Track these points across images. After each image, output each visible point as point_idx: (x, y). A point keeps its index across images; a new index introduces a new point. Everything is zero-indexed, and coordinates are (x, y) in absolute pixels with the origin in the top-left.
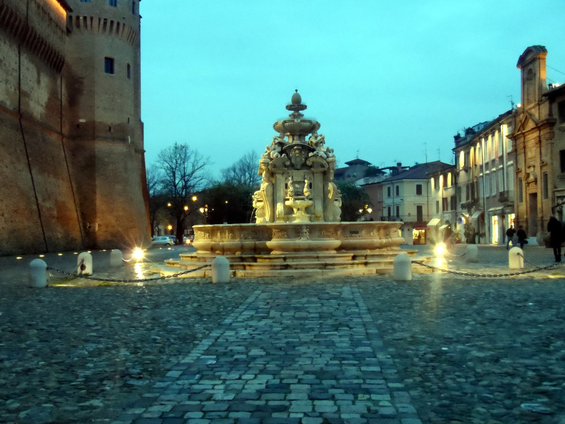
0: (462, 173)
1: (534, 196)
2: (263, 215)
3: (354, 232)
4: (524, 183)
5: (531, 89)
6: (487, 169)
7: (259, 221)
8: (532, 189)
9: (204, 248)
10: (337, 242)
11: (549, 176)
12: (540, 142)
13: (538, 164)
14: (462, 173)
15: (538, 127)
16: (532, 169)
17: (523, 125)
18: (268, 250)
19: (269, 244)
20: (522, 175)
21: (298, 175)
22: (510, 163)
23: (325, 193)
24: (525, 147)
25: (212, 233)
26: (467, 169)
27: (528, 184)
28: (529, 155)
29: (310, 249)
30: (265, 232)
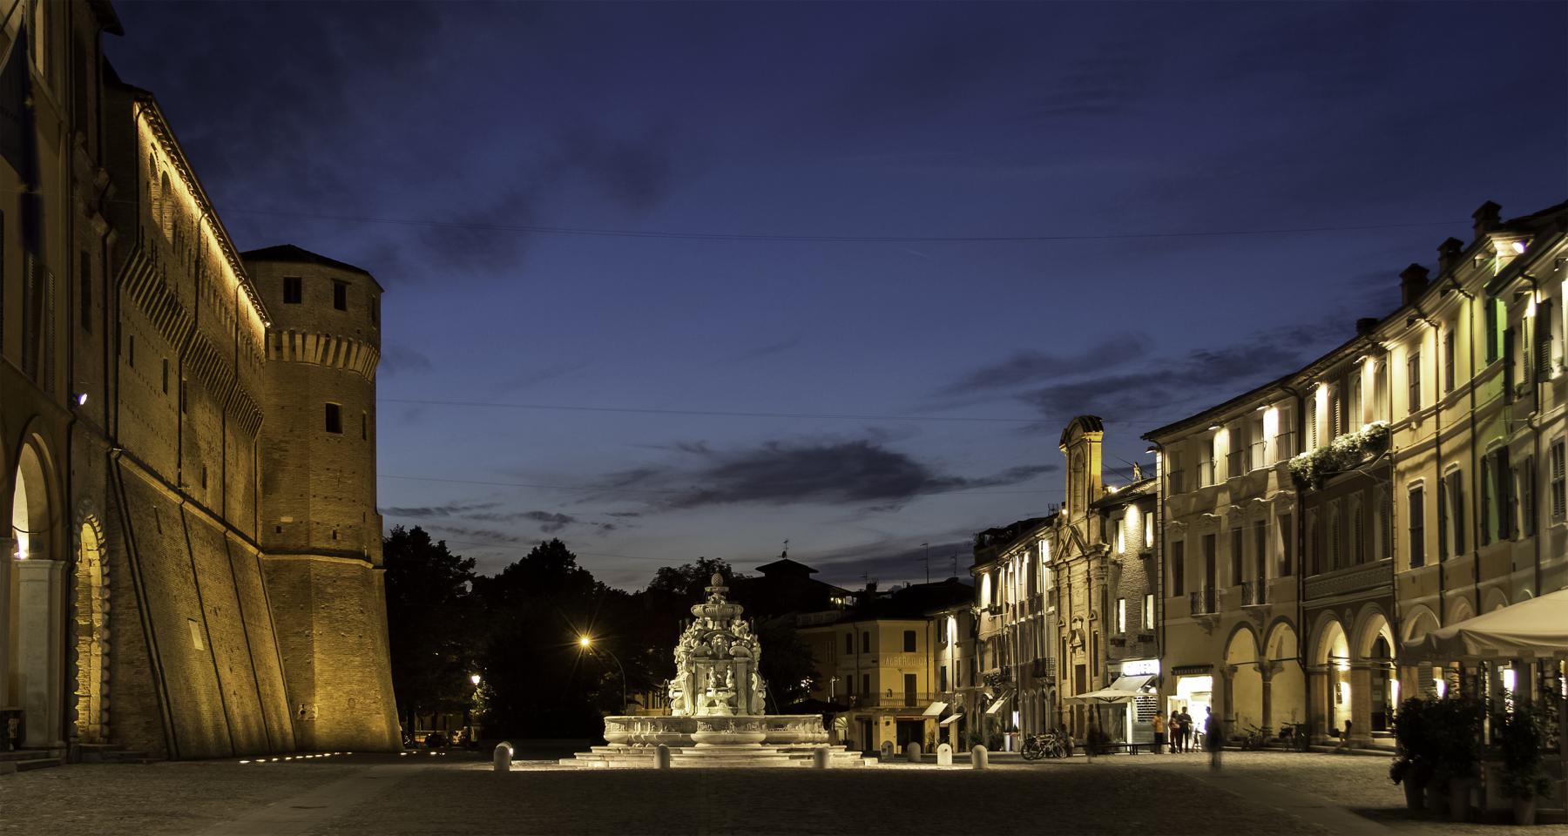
0: (986, 616)
1: (1081, 669)
2: (682, 707)
3: (779, 725)
4: (1068, 646)
5: (1080, 487)
6: (1022, 615)
7: (676, 713)
8: (1081, 658)
9: (620, 741)
10: (763, 736)
11: (1101, 639)
12: (1089, 580)
13: (1086, 621)
14: (986, 616)
15: (1085, 557)
16: (1078, 625)
17: (1067, 549)
18: (692, 744)
19: (693, 736)
20: (1066, 632)
21: (720, 666)
22: (1052, 609)
23: (749, 683)
24: (1070, 586)
25: (628, 725)
26: (995, 610)
27: (1074, 649)
28: (1077, 600)
29: (735, 743)
30: (687, 725)
